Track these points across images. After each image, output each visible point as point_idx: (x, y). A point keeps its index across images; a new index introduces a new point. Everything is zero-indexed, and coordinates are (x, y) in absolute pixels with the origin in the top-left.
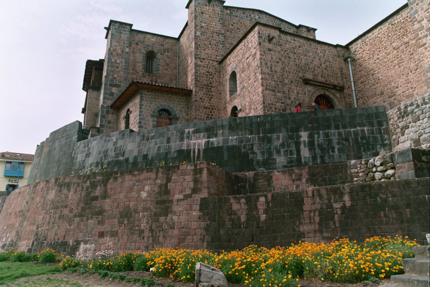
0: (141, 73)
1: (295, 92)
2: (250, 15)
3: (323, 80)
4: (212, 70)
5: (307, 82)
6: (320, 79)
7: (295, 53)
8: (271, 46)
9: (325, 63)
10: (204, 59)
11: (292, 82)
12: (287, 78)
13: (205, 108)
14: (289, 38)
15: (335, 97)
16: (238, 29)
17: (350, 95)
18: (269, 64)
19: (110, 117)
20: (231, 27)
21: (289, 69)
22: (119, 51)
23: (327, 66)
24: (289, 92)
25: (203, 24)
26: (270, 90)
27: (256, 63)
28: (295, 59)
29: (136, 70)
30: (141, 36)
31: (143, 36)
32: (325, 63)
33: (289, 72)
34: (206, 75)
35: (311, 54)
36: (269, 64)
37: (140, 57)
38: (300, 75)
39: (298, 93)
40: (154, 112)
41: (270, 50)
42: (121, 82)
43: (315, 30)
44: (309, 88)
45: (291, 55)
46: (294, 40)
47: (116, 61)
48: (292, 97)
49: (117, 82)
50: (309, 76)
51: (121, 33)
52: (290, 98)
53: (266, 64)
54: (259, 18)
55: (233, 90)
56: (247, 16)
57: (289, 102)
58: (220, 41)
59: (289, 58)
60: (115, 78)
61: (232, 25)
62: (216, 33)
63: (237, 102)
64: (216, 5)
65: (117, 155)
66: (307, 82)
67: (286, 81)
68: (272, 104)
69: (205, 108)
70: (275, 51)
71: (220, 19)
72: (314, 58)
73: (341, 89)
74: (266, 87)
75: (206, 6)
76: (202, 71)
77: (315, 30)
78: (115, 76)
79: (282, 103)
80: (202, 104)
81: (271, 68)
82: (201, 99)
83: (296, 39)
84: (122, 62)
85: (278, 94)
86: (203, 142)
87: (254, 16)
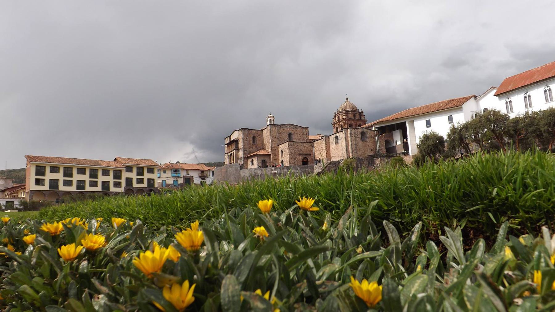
4: (276, 148)
5: (300, 155)
8: (291, 147)
15: (308, 157)
17: (313, 156)
19: (245, 160)
22: (246, 139)
27: (288, 151)
30: (251, 131)
37: (251, 139)
43: (308, 127)
44: (301, 156)
50: (301, 153)
55: (282, 155)
63: (283, 159)
65: (255, 174)
66: (300, 155)
73: (310, 155)
74: (290, 158)
77: (308, 127)
86: (276, 172)
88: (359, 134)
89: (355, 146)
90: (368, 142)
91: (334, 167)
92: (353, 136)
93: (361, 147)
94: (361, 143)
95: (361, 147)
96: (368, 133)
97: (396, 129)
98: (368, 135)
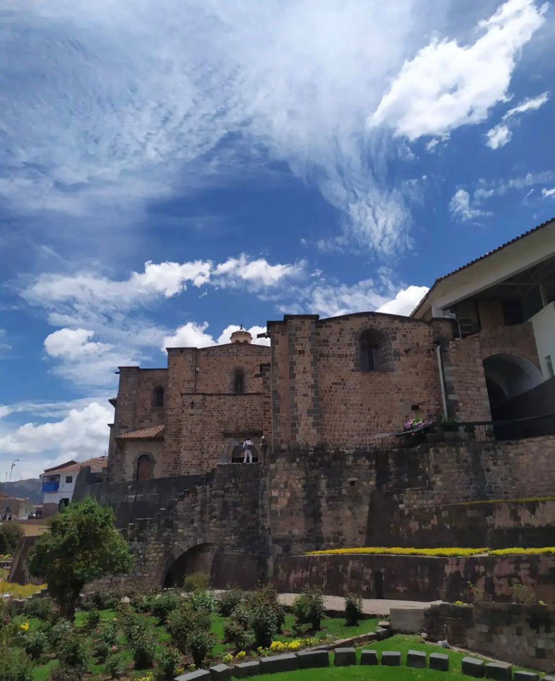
0: (149, 409)
1: (215, 447)
2: (228, 350)
3: (247, 429)
5: (226, 435)
6: (242, 429)
7: (219, 411)
8: (192, 411)
9: (250, 413)
10: (174, 408)
11: (212, 438)
12: (208, 435)
13: (174, 452)
14: (214, 398)
16: (214, 368)
18: (189, 428)
20: (208, 368)
21: (211, 427)
22: (127, 395)
23: (252, 415)
24: (208, 447)
25: (175, 376)
26: (187, 450)
28: (218, 416)
29: (145, 408)
30: (150, 373)
31: (152, 372)
32: (250, 413)
33: (211, 430)
34: (175, 423)
35: (235, 408)
36: (189, 428)
38: (222, 429)
39: (217, 446)
40: (135, 459)
41: (191, 415)
42: (128, 423)
45: (215, 413)
46: (219, 399)
47: (124, 404)
48: (211, 453)
49: (125, 424)
50: (232, 428)
51: (128, 377)
52: (208, 452)
53: (187, 428)
54: (238, 350)
56: (224, 353)
57: (207, 456)
58: (190, 388)
59: (213, 416)
60: (123, 420)
61: (208, 366)
62: (187, 381)
64: (189, 353)
67: (207, 438)
68: (189, 462)
69: (174, 452)
70: (197, 415)
71: (191, 366)
72: (239, 410)
75: (179, 356)
76: (172, 420)
78: (123, 418)
79: (198, 459)
80: (171, 450)
81: (191, 431)
82: (170, 445)
83: (221, 397)
84: (129, 404)
85: (196, 452)
86: (133, 497)
87: (233, 350)
88: (347, 338)
89: (311, 394)
90: (399, 372)
91: (227, 490)
92: (302, 352)
93: (355, 399)
94: (355, 379)
95: (355, 399)
96: (399, 336)
97: (543, 304)
98: (395, 345)
